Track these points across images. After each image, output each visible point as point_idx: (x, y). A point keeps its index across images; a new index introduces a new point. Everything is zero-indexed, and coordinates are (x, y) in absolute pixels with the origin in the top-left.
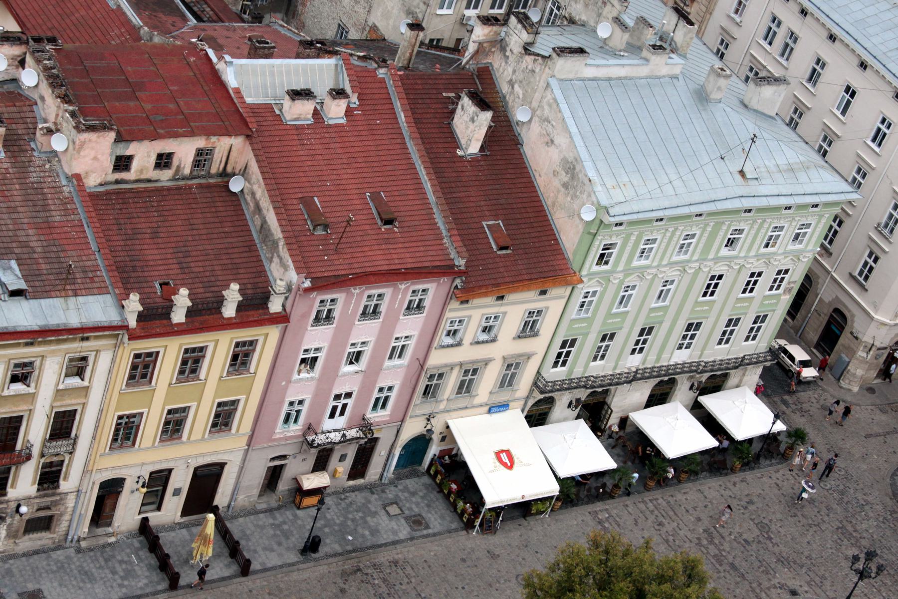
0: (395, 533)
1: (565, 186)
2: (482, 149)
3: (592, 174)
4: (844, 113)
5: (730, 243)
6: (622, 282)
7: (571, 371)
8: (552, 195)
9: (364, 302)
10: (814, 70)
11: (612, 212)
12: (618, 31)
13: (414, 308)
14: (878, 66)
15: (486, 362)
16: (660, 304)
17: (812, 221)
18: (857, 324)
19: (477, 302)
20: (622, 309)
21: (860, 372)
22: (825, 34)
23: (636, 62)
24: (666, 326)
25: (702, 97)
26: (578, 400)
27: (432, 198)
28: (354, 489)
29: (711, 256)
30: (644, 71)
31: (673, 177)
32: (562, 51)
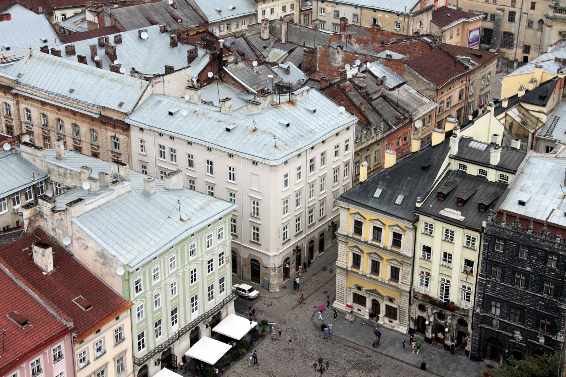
1: (103, 264)
2: (55, 266)
3: (113, 253)
4: (211, 173)
5: (192, 253)
6: (152, 295)
7: (148, 348)
8: (99, 271)
9: (31, 368)
10: (189, 160)
11: (131, 265)
12: (93, 183)
13: (58, 357)
14: (216, 147)
15: (106, 365)
16: (174, 296)
17: (222, 226)
18: (264, 261)
19: (87, 339)
20: (158, 307)
21: (276, 282)
22: (186, 143)
23: (108, 193)
24: (182, 304)
25: (146, 194)
26: (158, 360)
27: (41, 301)
29: (186, 263)
30: (114, 195)
31: (152, 236)
32: (71, 204)
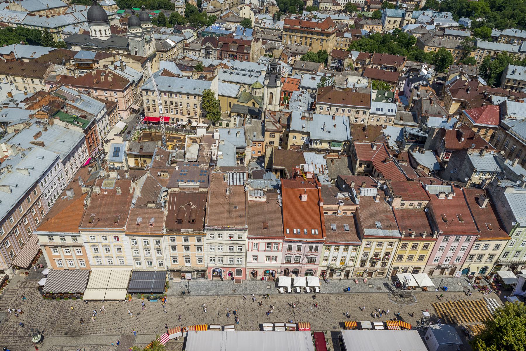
0: (460, 289)
28: (450, 277)
